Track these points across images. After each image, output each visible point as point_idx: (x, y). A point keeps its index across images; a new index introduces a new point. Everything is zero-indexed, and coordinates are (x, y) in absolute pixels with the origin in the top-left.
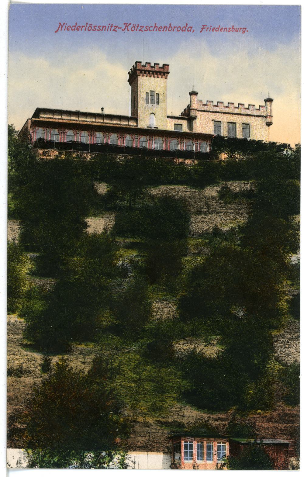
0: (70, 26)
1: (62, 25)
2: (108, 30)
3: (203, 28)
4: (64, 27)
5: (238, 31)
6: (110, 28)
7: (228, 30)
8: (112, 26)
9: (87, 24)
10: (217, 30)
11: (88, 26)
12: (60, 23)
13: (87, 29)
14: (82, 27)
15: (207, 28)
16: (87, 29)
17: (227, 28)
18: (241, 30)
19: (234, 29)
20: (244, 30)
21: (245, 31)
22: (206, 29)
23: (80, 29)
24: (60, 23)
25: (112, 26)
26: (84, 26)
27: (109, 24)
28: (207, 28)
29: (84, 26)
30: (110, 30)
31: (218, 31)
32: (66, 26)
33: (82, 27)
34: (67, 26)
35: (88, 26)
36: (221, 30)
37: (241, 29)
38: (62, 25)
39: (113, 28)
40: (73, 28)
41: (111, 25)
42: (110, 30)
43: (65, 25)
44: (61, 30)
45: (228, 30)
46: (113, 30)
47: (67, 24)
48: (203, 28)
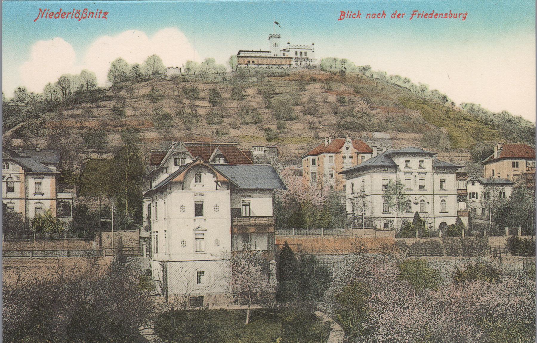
0: (53, 13)
1: (43, 11)
2: (96, 17)
3: (413, 15)
4: (45, 13)
5: (456, 17)
6: (98, 14)
7: (444, 16)
8: (100, 13)
9: (74, 10)
10: (430, 16)
11: (75, 12)
12: (40, 9)
13: (73, 16)
14: (69, 13)
15: (419, 14)
16: (73, 16)
17: (442, 14)
18: (461, 16)
19: (452, 14)
20: (464, 16)
21: (465, 17)
22: (417, 15)
23: (66, 16)
24: (40, 9)
25: (100, 13)
26: (70, 13)
27: (98, 10)
28: (419, 14)
29: (70, 13)
30: (99, 17)
31: (431, 17)
32: (47, 13)
33: (69, 13)
34: (49, 12)
35: (75, 12)
36: (435, 16)
37: (460, 14)
38: (43, 11)
39: (102, 15)
40: (57, 16)
41: (99, 11)
42: (99, 17)
43: (47, 11)
44: (42, 17)
45: (444, 16)
46: (103, 17)
47: (48, 10)
48: (413, 15)
